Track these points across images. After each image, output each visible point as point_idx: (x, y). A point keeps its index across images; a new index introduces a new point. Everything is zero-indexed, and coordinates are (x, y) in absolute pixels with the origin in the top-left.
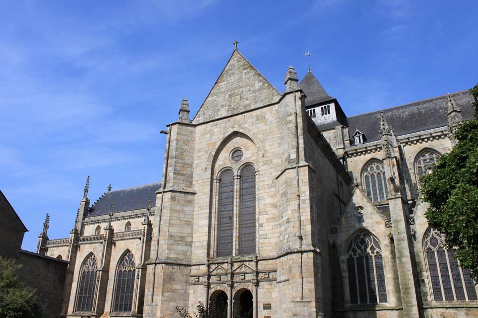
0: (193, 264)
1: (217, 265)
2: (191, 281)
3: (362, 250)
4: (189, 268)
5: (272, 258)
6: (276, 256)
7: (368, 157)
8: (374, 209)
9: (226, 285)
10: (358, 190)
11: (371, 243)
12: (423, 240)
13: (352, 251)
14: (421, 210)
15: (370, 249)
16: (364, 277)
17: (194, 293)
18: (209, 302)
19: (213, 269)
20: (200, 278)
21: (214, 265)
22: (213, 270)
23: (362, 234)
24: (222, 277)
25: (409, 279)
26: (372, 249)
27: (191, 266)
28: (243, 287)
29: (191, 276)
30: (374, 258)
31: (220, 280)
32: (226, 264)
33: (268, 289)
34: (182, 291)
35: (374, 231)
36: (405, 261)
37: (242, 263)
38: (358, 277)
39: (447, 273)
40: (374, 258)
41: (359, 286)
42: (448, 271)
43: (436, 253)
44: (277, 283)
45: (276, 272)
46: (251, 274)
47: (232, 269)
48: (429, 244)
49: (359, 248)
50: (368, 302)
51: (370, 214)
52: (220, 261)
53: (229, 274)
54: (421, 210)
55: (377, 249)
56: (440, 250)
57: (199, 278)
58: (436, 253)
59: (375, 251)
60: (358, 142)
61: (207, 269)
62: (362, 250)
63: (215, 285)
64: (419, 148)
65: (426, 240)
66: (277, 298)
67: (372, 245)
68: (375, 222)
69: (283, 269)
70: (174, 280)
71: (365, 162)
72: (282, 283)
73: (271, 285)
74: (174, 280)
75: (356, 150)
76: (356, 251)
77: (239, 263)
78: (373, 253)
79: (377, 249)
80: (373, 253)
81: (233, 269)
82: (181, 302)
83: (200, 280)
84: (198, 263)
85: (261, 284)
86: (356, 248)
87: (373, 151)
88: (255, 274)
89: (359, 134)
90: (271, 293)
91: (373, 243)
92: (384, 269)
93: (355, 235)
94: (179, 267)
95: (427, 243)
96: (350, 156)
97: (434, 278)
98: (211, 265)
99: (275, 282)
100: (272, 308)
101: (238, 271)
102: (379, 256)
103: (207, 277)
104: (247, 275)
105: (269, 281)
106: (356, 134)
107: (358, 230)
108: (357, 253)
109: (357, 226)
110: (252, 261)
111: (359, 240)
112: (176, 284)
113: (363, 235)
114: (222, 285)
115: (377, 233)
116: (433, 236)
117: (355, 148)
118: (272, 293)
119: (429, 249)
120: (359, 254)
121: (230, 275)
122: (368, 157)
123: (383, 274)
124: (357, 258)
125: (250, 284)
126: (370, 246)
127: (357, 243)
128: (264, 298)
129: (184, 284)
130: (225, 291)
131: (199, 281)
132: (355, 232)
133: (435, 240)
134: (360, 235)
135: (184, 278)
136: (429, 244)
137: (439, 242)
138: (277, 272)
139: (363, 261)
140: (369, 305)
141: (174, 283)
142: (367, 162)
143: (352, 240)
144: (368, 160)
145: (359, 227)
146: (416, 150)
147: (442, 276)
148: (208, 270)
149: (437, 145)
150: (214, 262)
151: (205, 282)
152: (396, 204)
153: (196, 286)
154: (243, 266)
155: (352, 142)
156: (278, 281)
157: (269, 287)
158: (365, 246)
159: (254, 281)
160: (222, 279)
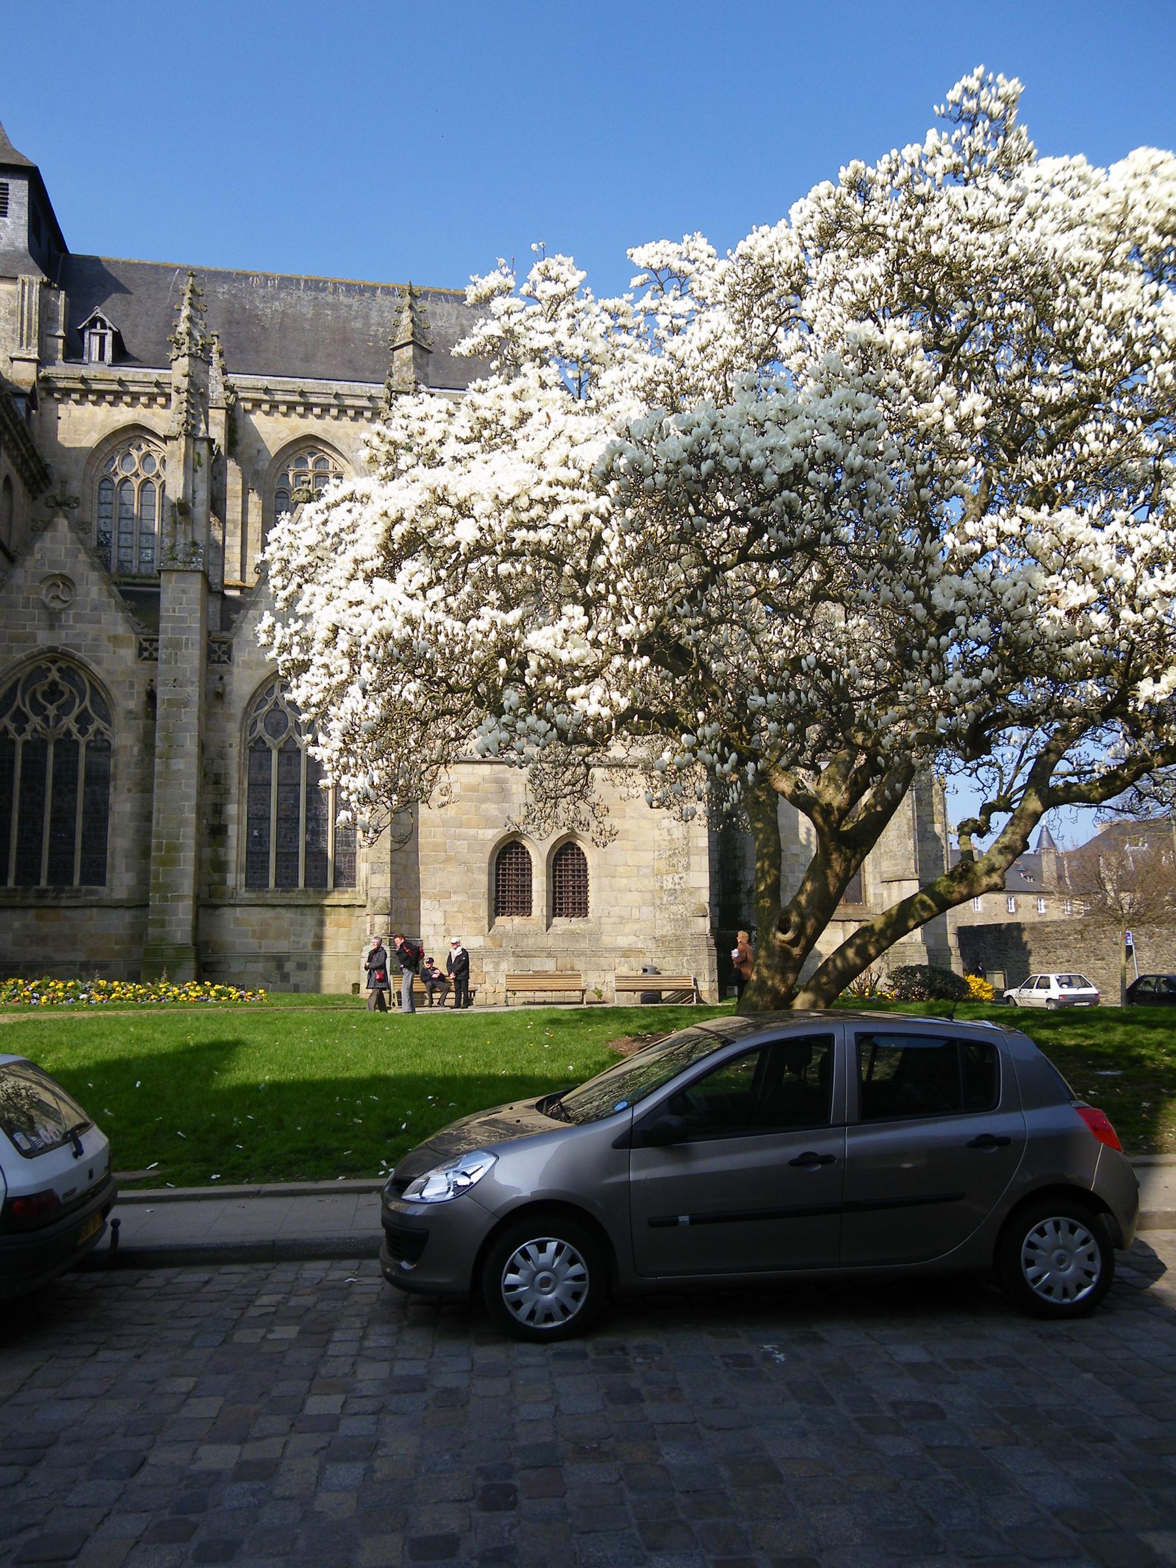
3: (46, 719)
7: (123, 415)
8: (111, 595)
10: (65, 522)
11: (82, 701)
12: (246, 712)
13: (13, 720)
15: (77, 720)
16: (41, 805)
23: (54, 668)
25: (182, 823)
26: (83, 720)
36: (182, 767)
38: (22, 803)
39: (293, 813)
40: (82, 750)
41: (20, 830)
48: (260, 726)
49: (39, 709)
50: (43, 883)
51: (95, 609)
55: (98, 723)
59: (91, 729)
60: (95, 355)
62: (46, 719)
64: (292, 430)
65: (254, 715)
67: (86, 708)
71: (108, 431)
75: (83, 380)
76: (27, 720)
78: (83, 731)
79: (98, 723)
80: (83, 731)
86: (27, 710)
87: (143, 400)
89: (104, 326)
91: (87, 702)
92: (112, 784)
93: (29, 669)
95: (255, 723)
96: (56, 395)
97: (257, 819)
102: (102, 747)
106: (93, 324)
107: (42, 652)
108: (28, 727)
109: (44, 639)
111: (42, 686)
113: (60, 670)
115: (108, 672)
117: (84, 371)
119: (261, 740)
120: (35, 730)
122: (123, 415)
123: (106, 802)
124: (26, 743)
126: (76, 711)
127: (34, 692)
132: (31, 657)
133: (278, 715)
134: (49, 670)
136: (260, 726)
139: (45, 755)
140: (46, 891)
142: (115, 434)
143: (19, 680)
144: (119, 425)
145: (49, 644)
146: (282, 436)
147: (278, 819)
149: (348, 435)
152: (184, 592)
155: (74, 352)
158: (58, 708)
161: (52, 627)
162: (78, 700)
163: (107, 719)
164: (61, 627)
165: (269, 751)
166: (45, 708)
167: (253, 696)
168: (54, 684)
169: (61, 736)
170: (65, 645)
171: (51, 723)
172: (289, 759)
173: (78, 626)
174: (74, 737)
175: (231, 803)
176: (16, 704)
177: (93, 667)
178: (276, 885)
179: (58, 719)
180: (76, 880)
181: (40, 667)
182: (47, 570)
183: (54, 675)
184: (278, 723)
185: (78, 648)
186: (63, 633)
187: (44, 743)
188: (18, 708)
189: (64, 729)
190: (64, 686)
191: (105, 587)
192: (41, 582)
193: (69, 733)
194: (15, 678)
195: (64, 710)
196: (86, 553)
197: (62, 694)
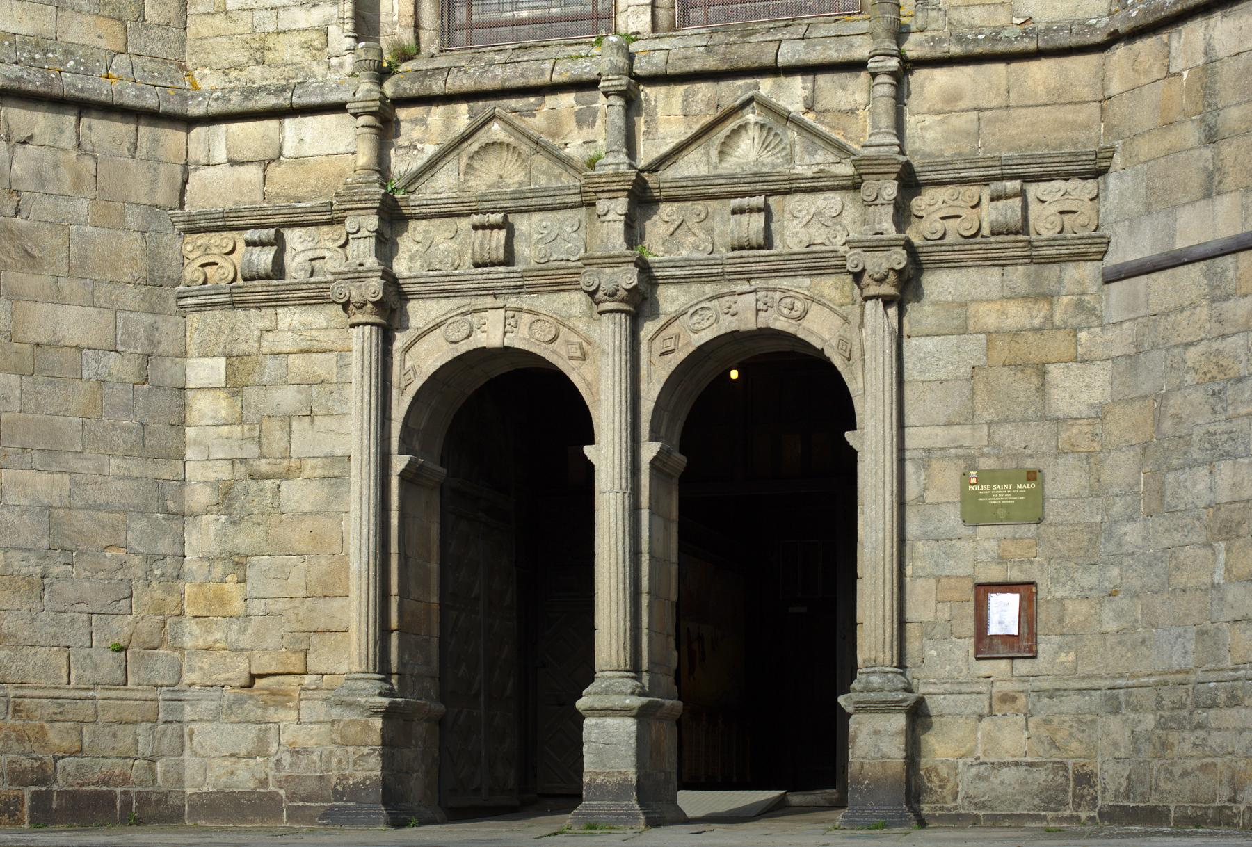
0: (215, 108)
1: (462, 116)
2: (192, 272)
4: (172, 138)
5: (1064, 40)
6: (1102, 26)
9: (575, 302)
17: (234, 387)
18: (399, 463)
19: (430, 149)
20: (293, 237)
21: (436, 115)
22: (432, 165)
24: (523, 224)
27: (189, 122)
28: (748, 323)
29: (192, 228)
31: (509, 259)
32: (567, 101)
33: (1016, 333)
34: (119, 367)
37: (735, 90)
44: (1114, 276)
45: (1099, 173)
46: (834, 201)
47: (631, 150)
52: (500, 76)
53: (612, 193)
57: (279, 242)
61: (365, 156)
63: (453, 303)
66: (1101, 413)
69: (1212, 137)
70: (31, 260)
72: (1195, 271)
73: (1049, 297)
74: (31, 260)
77: (704, 90)
81: (647, 153)
82: (115, 465)
83: (295, 264)
84: (270, 101)
85: (938, 285)
88: (890, 189)
90: (1041, 370)
94: (71, 119)
98: (402, 114)
99: (1084, 274)
100: (1053, 511)
101: (693, 166)
103: (372, 222)
104: (793, 201)
105: (1032, 260)
110: (856, 66)
112: (58, 298)
114: (527, 301)
118: (1055, 372)
121: (621, 205)
125: (829, 287)
128: (969, 417)
129: (130, 297)
130: (558, 357)
131: (278, 269)
135: (133, 244)
138: (1112, 179)
141: (32, 282)
148: (382, 166)
150: (437, 87)
151: (357, 275)
153: (257, 319)
154: (751, 117)
156: (1120, 254)
157: (1017, 315)
159: (877, 263)
160: (521, 249)
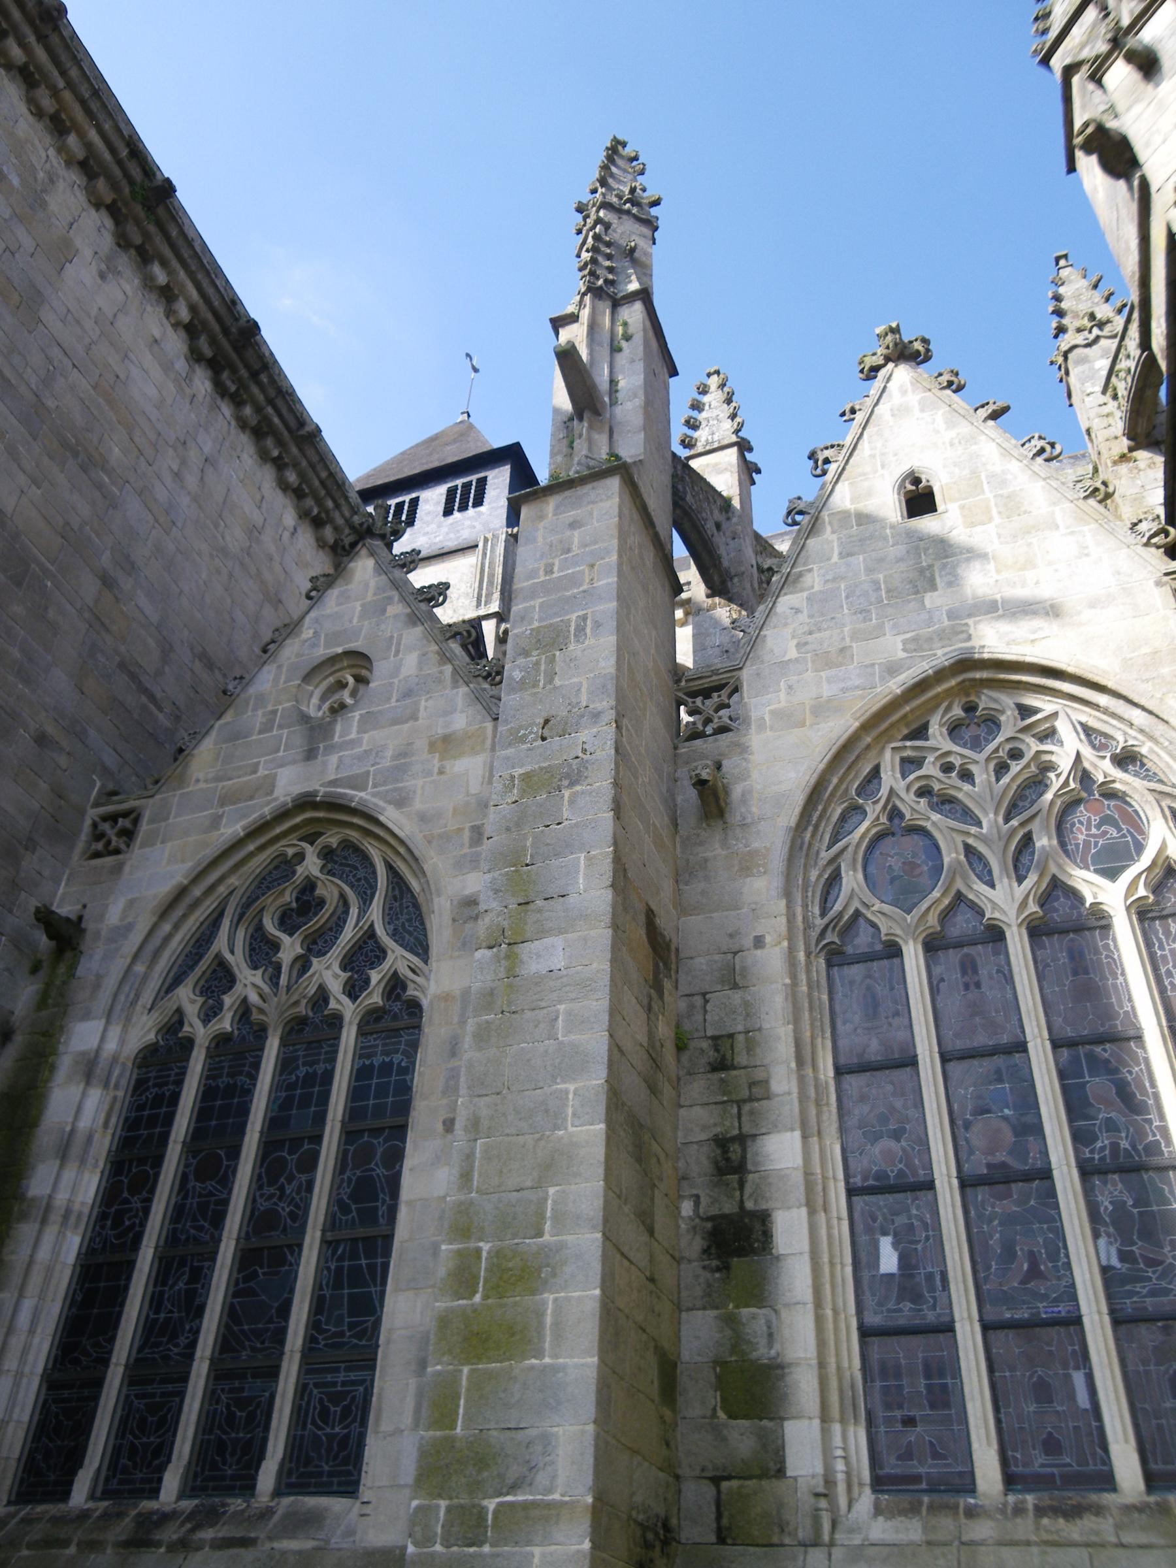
8: (445, 658)
11: (363, 912)
14: (803, 617)
30: (349, 1037)
35: (401, 802)
36: (558, 961)
39: (1019, 1151)
40: (349, 1037)
42: (1037, 1129)
43: (913, 957)
48: (852, 880)
54: (803, 617)
55: (398, 958)
56: (962, 924)
58: (913, 957)
68: (421, 744)
78: (353, 990)
79: (398, 958)
91: (376, 912)
95: (835, 879)
107: (283, 815)
113: (327, 854)
115: (423, 818)
116: (895, 814)
126: (349, 935)
134: (300, 857)
137: (951, 855)
145: (298, 789)
152: (574, 525)
161: (310, 754)
162: (354, 912)
163: (421, 948)
164: (330, 749)
165: (893, 951)
166: (276, 946)
167: (815, 795)
168: (310, 885)
169: (302, 1009)
170: (333, 783)
171: (283, 980)
172: (969, 967)
173: (366, 736)
174: (333, 1004)
175: (775, 1128)
176: (214, 949)
177: (390, 816)
178: (1010, 1480)
179: (303, 964)
180: (267, 1476)
181: (284, 855)
182: (322, 652)
183: (312, 865)
184: (911, 866)
185: (358, 782)
186: (333, 759)
187: (261, 1032)
188: (218, 956)
189: (312, 990)
190: (329, 890)
191: (435, 648)
192: (307, 678)
193: (322, 996)
194: (222, 890)
195: (317, 945)
196: (403, 598)
197: (321, 902)
